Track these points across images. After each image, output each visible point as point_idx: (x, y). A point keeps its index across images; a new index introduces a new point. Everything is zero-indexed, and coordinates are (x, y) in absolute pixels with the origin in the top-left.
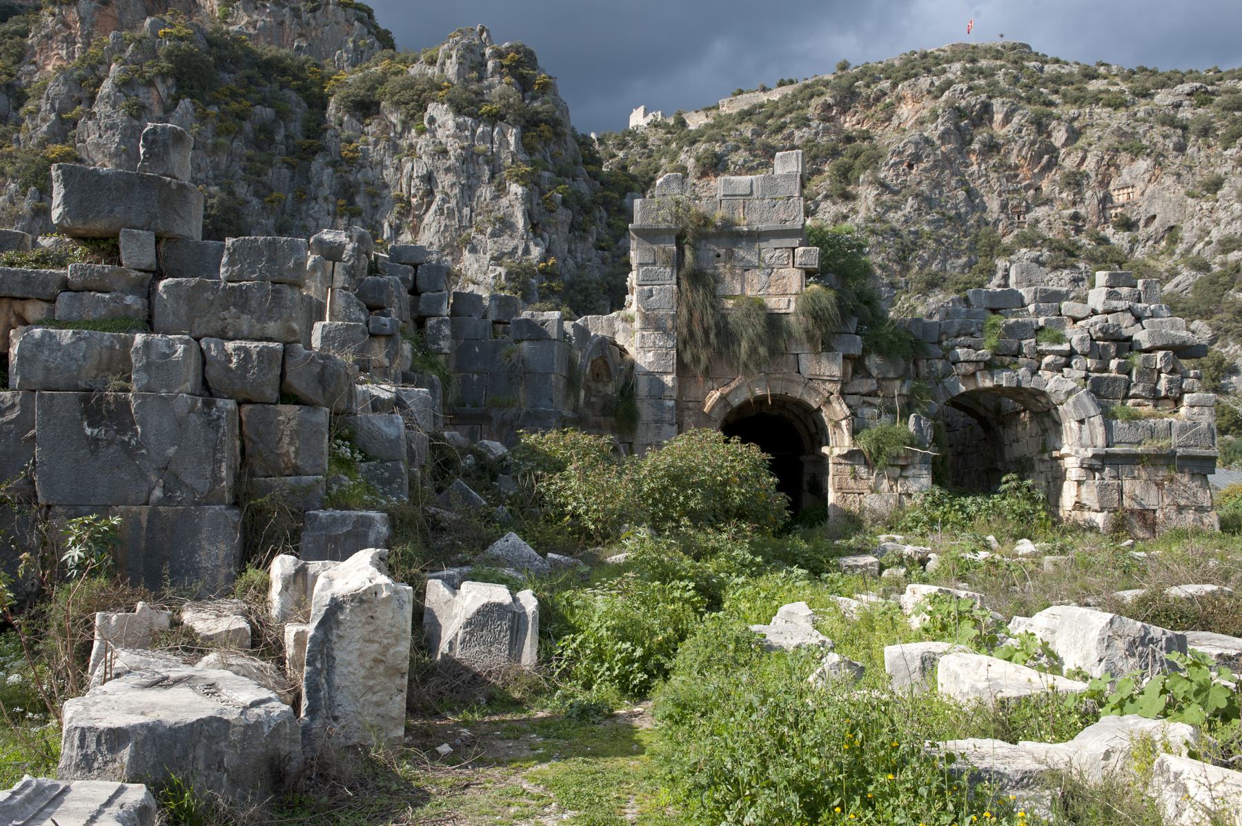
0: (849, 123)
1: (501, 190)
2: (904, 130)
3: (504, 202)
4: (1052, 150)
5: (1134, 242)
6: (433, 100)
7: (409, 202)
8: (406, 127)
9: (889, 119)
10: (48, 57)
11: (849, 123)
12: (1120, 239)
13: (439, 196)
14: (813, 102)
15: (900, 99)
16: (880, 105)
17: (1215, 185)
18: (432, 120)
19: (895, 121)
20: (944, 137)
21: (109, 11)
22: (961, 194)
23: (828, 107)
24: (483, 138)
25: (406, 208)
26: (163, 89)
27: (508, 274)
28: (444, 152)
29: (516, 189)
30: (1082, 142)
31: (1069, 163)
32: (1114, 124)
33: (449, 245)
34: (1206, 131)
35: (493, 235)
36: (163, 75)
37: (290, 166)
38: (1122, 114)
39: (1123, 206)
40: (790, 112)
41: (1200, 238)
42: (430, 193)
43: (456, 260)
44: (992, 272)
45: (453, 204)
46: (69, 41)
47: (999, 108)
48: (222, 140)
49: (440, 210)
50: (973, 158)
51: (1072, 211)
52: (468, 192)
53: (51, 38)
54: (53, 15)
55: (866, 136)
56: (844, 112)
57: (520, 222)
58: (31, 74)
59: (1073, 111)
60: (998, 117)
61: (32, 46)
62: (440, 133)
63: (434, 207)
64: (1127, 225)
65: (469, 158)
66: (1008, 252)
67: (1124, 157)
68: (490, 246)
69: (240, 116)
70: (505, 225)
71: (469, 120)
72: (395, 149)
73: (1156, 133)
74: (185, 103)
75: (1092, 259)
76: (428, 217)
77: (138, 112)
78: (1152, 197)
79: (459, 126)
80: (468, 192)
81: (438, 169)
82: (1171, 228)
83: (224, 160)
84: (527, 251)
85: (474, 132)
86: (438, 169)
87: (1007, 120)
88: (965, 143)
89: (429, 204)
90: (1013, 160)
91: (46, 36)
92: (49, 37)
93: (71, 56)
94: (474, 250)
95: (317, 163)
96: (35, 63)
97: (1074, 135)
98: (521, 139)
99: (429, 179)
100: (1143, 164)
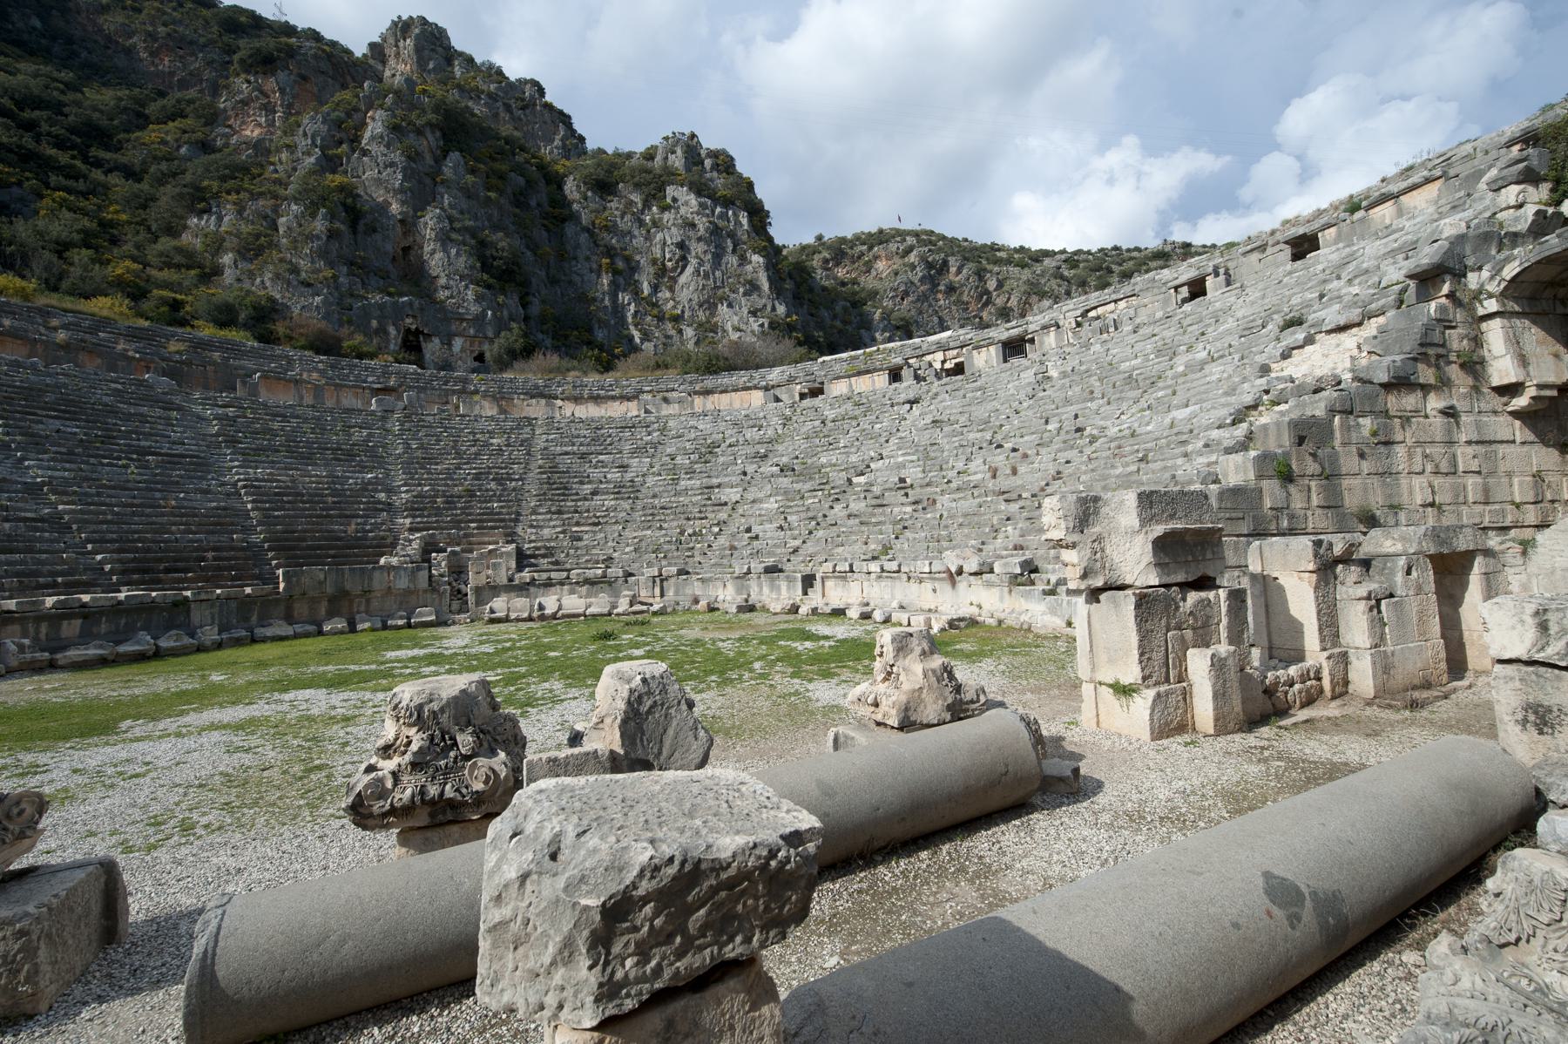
0: (841, 273)
1: (743, 260)
3: (749, 268)
4: (987, 292)
7: (663, 264)
8: (647, 205)
10: (243, 123)
11: (841, 273)
13: (693, 261)
14: (816, 257)
15: (876, 258)
16: (861, 262)
18: (675, 200)
19: (874, 273)
20: (922, 280)
22: (936, 319)
23: (826, 261)
24: (721, 216)
25: (662, 271)
26: (431, 140)
27: (771, 324)
28: (693, 226)
29: (757, 259)
30: (1006, 288)
31: (1000, 301)
32: (1024, 278)
33: (707, 301)
35: (745, 294)
36: (430, 124)
37: (548, 230)
38: (1026, 271)
42: (684, 258)
43: (713, 315)
45: (707, 267)
46: (269, 109)
47: (953, 263)
48: (492, 195)
49: (697, 272)
50: (940, 296)
52: (717, 258)
53: (247, 104)
54: (248, 82)
55: (855, 282)
56: (837, 264)
57: (765, 286)
58: (228, 136)
59: (996, 269)
60: (953, 270)
61: (225, 110)
62: (683, 211)
63: (689, 270)
65: (715, 231)
67: (1034, 298)
68: (745, 304)
69: (502, 177)
70: (753, 287)
72: (641, 223)
73: (1054, 283)
74: (455, 156)
76: (683, 279)
77: (413, 156)
79: (701, 205)
80: (717, 258)
81: (689, 238)
84: (774, 309)
85: (713, 212)
86: (689, 238)
87: (959, 272)
88: (935, 285)
89: (684, 268)
90: (965, 298)
91: (241, 101)
92: (245, 103)
93: (271, 123)
94: (730, 306)
95: (570, 229)
96: (230, 126)
97: (1000, 285)
98: (750, 221)
99: (681, 245)
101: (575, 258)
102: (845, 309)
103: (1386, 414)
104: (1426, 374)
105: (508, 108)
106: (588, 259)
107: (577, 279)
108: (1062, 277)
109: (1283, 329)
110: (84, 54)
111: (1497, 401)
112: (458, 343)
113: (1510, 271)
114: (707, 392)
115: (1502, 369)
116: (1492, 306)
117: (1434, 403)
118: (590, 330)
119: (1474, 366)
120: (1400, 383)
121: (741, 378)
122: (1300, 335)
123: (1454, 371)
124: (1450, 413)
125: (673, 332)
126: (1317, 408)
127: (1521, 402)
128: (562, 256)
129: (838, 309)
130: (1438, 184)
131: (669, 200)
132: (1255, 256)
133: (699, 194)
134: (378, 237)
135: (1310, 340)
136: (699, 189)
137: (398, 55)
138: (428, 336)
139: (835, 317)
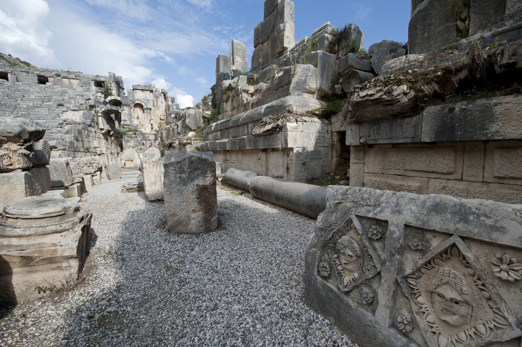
103: (88, 130)
104: (93, 125)
109: (58, 106)
111: (100, 131)
113: (103, 109)
115: (101, 126)
116: (100, 114)
117: (93, 130)
119: (97, 124)
120: (90, 126)
122: (62, 109)
123: (96, 125)
124: (95, 132)
126: (80, 127)
127: (103, 132)
130: (78, 81)
132: (25, 74)
135: (67, 111)
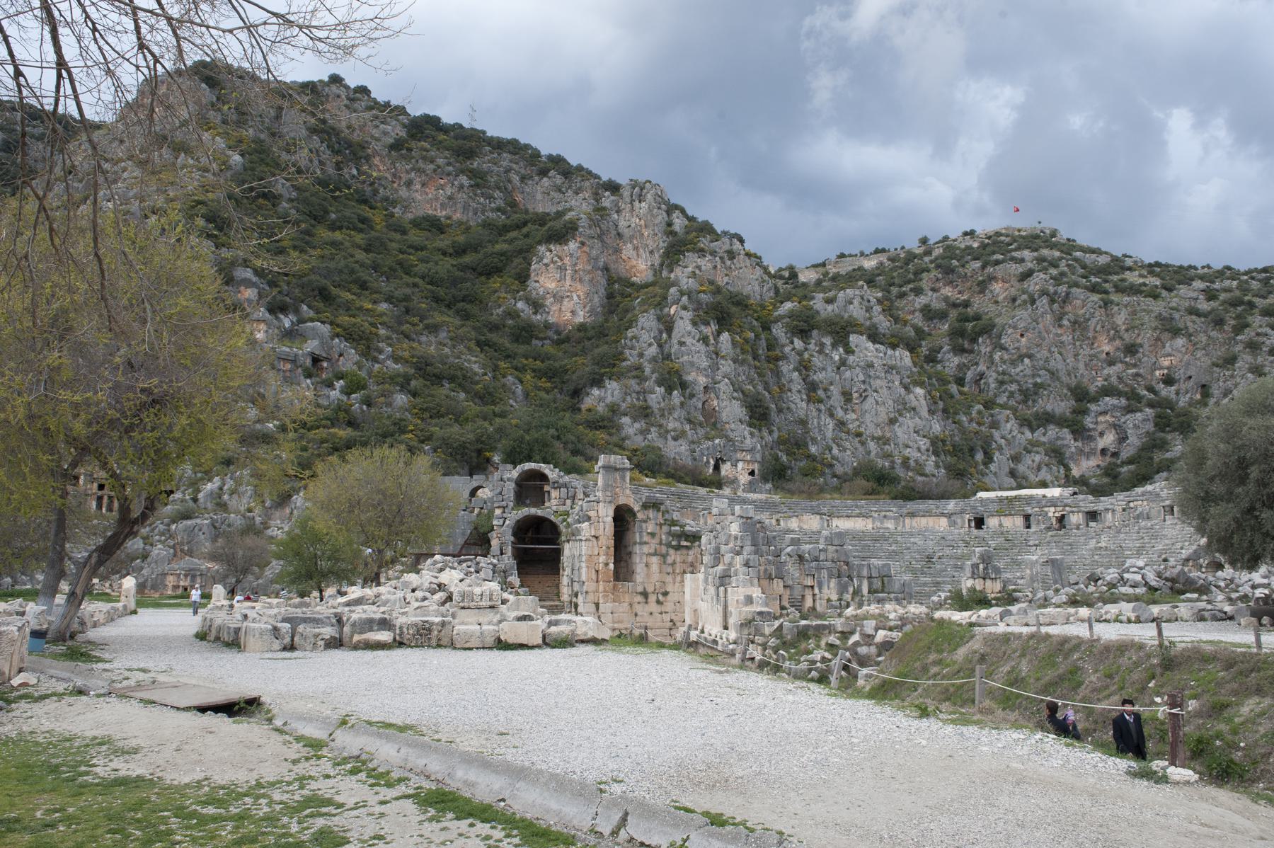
2: (996, 302)
5: (1177, 393)
6: (854, 332)
9: (982, 292)
12: (1166, 392)
17: (1230, 361)
21: (586, 249)
34: (1219, 323)
39: (1168, 368)
40: (909, 282)
41: (1225, 395)
44: (1085, 412)
46: (562, 269)
51: (1134, 371)
55: (966, 304)
64: (1169, 381)
66: (1095, 400)
67: (1166, 335)
71: (882, 347)
75: (1151, 405)
78: (1188, 364)
82: (1203, 386)
83: (746, 368)
100: (1180, 342)
101: (790, 390)
102: (979, 412)
105: (721, 258)
106: (799, 392)
107: (793, 406)
108: (1198, 313)
110: (382, 190)
112: (740, 465)
114: (912, 515)
118: (806, 445)
121: (930, 504)
125: (858, 445)
128: (782, 388)
129: (974, 414)
131: (852, 345)
133: (874, 342)
134: (695, 400)
136: (874, 337)
137: (632, 210)
138: (724, 462)
139: (972, 420)
